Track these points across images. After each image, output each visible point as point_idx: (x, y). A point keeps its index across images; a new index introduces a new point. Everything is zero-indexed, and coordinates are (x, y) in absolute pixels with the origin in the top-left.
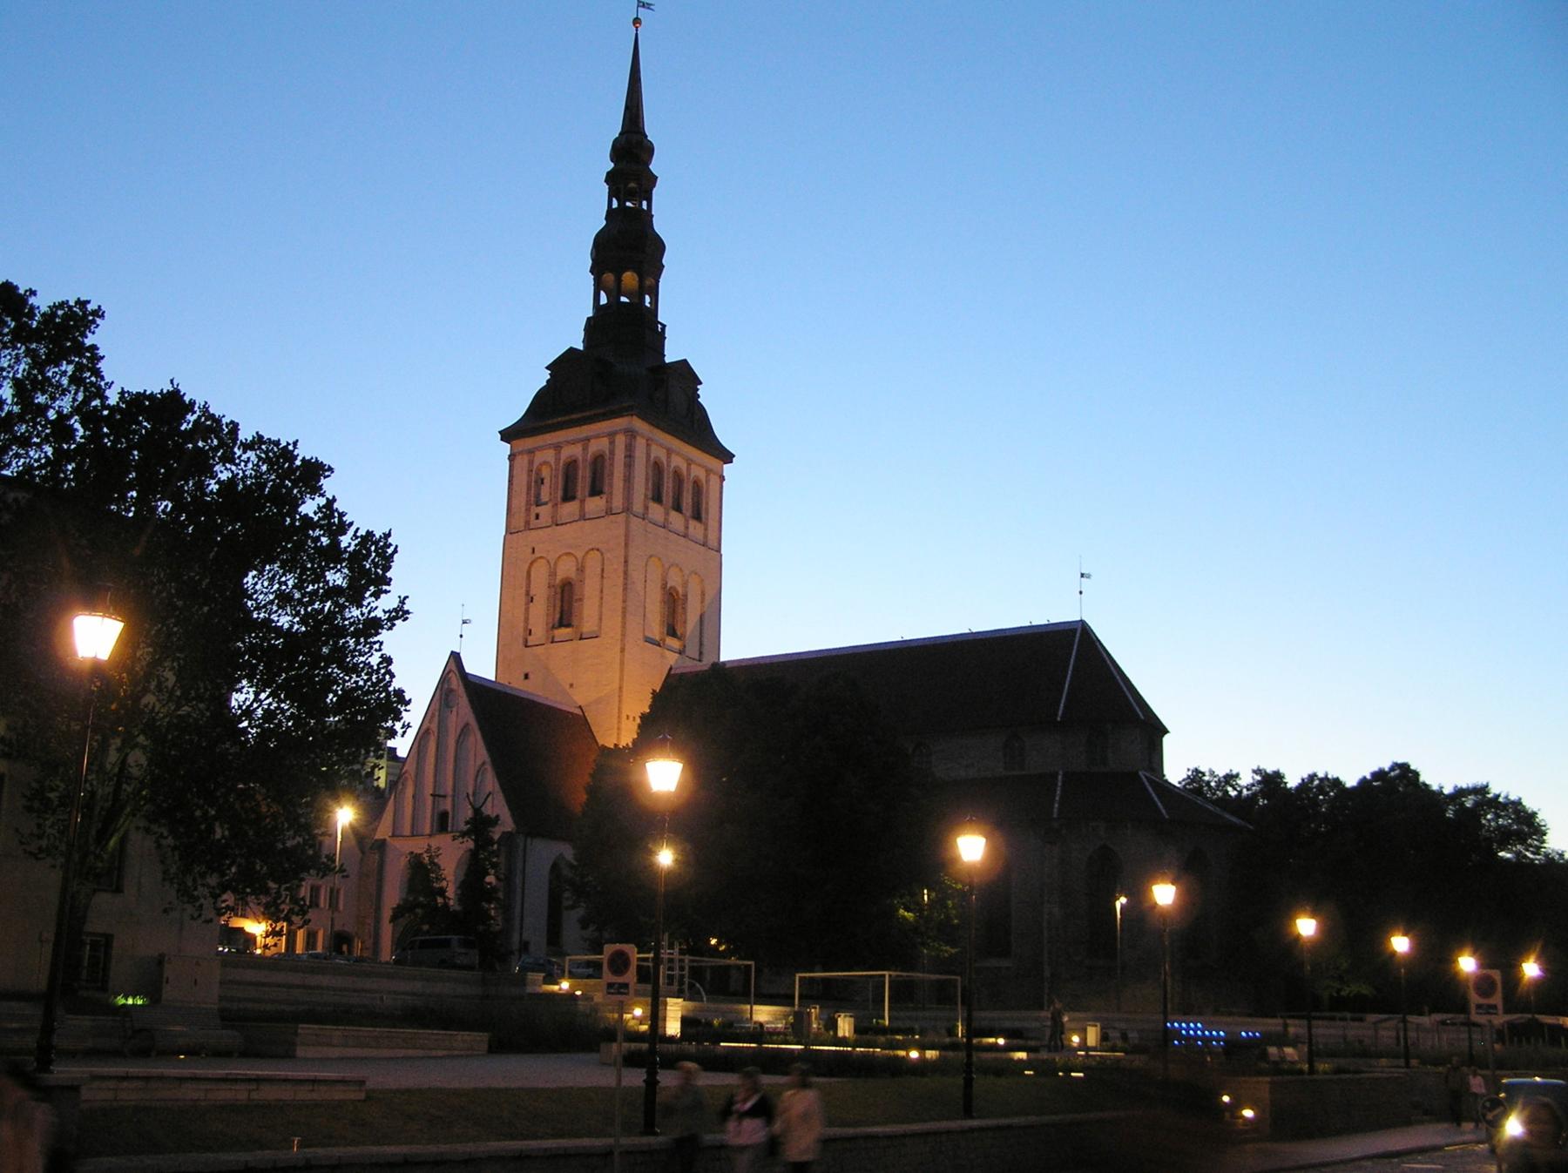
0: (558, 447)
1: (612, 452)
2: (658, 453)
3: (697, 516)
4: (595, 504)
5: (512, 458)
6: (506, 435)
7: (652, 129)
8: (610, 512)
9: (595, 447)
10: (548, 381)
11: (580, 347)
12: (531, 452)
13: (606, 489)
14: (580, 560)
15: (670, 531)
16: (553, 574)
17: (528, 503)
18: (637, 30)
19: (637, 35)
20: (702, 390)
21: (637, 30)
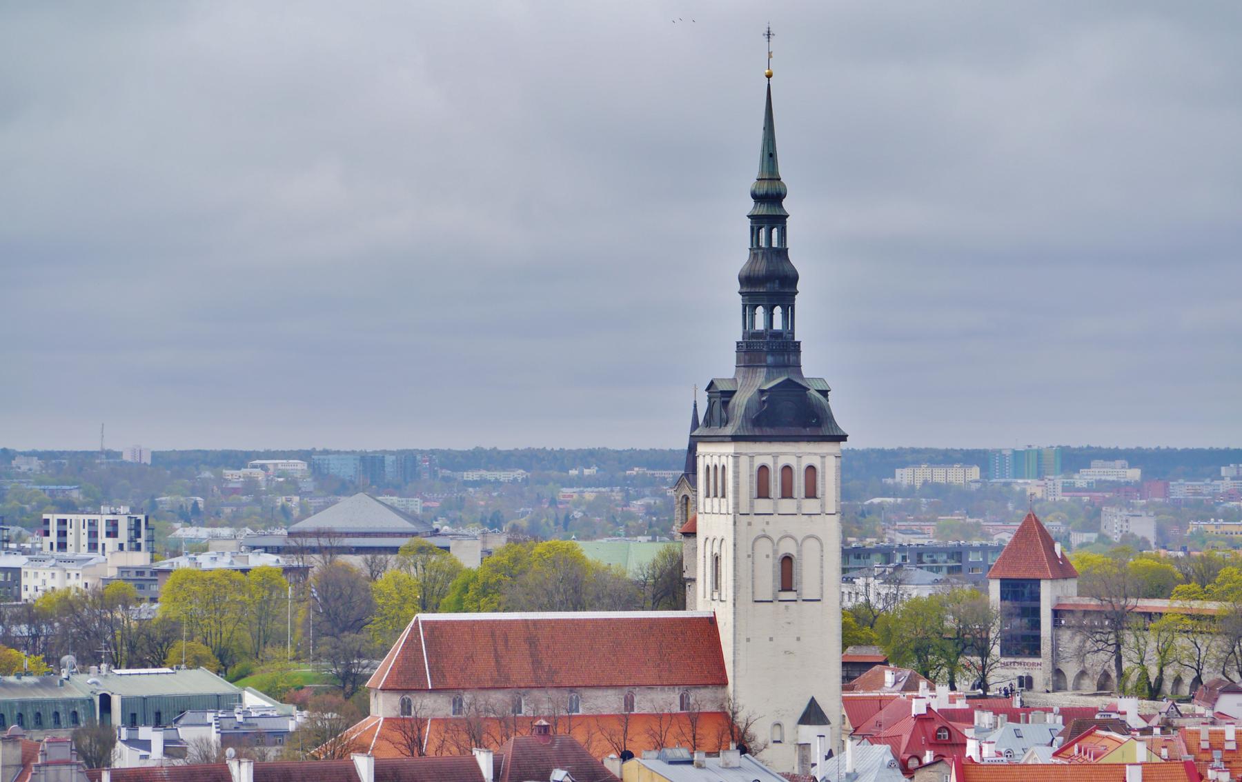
0: (775, 456)
4: (811, 505)
8: (823, 512)
13: (819, 494)
14: (799, 542)
16: (775, 552)
19: (769, 84)
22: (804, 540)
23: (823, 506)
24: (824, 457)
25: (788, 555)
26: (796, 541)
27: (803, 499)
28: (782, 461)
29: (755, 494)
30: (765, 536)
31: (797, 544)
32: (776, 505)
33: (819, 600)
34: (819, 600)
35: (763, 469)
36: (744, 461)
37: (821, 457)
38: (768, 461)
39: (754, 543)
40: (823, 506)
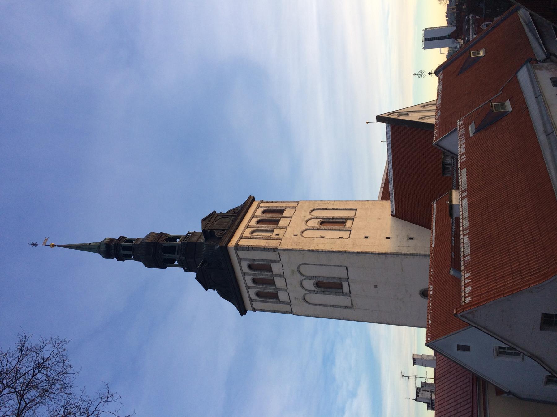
0: (248, 287)
1: (246, 260)
2: (247, 233)
3: (281, 211)
4: (276, 268)
5: (254, 310)
6: (243, 311)
7: (98, 238)
9: (246, 270)
10: (214, 290)
11: (194, 274)
12: (251, 300)
14: (304, 278)
15: (288, 226)
17: (277, 303)
18: (55, 246)
19: (57, 246)
20: (218, 212)
21: (55, 246)
22: (302, 275)
23: (275, 261)
24: (240, 258)
25: (315, 283)
26: (302, 280)
27: (272, 273)
28: (250, 284)
29: (275, 300)
30: (304, 299)
31: (304, 279)
32: (281, 290)
33: (347, 268)
34: (347, 268)
35: (258, 294)
36: (255, 305)
37: (241, 261)
38: (252, 292)
39: (309, 303)
40: (275, 261)
